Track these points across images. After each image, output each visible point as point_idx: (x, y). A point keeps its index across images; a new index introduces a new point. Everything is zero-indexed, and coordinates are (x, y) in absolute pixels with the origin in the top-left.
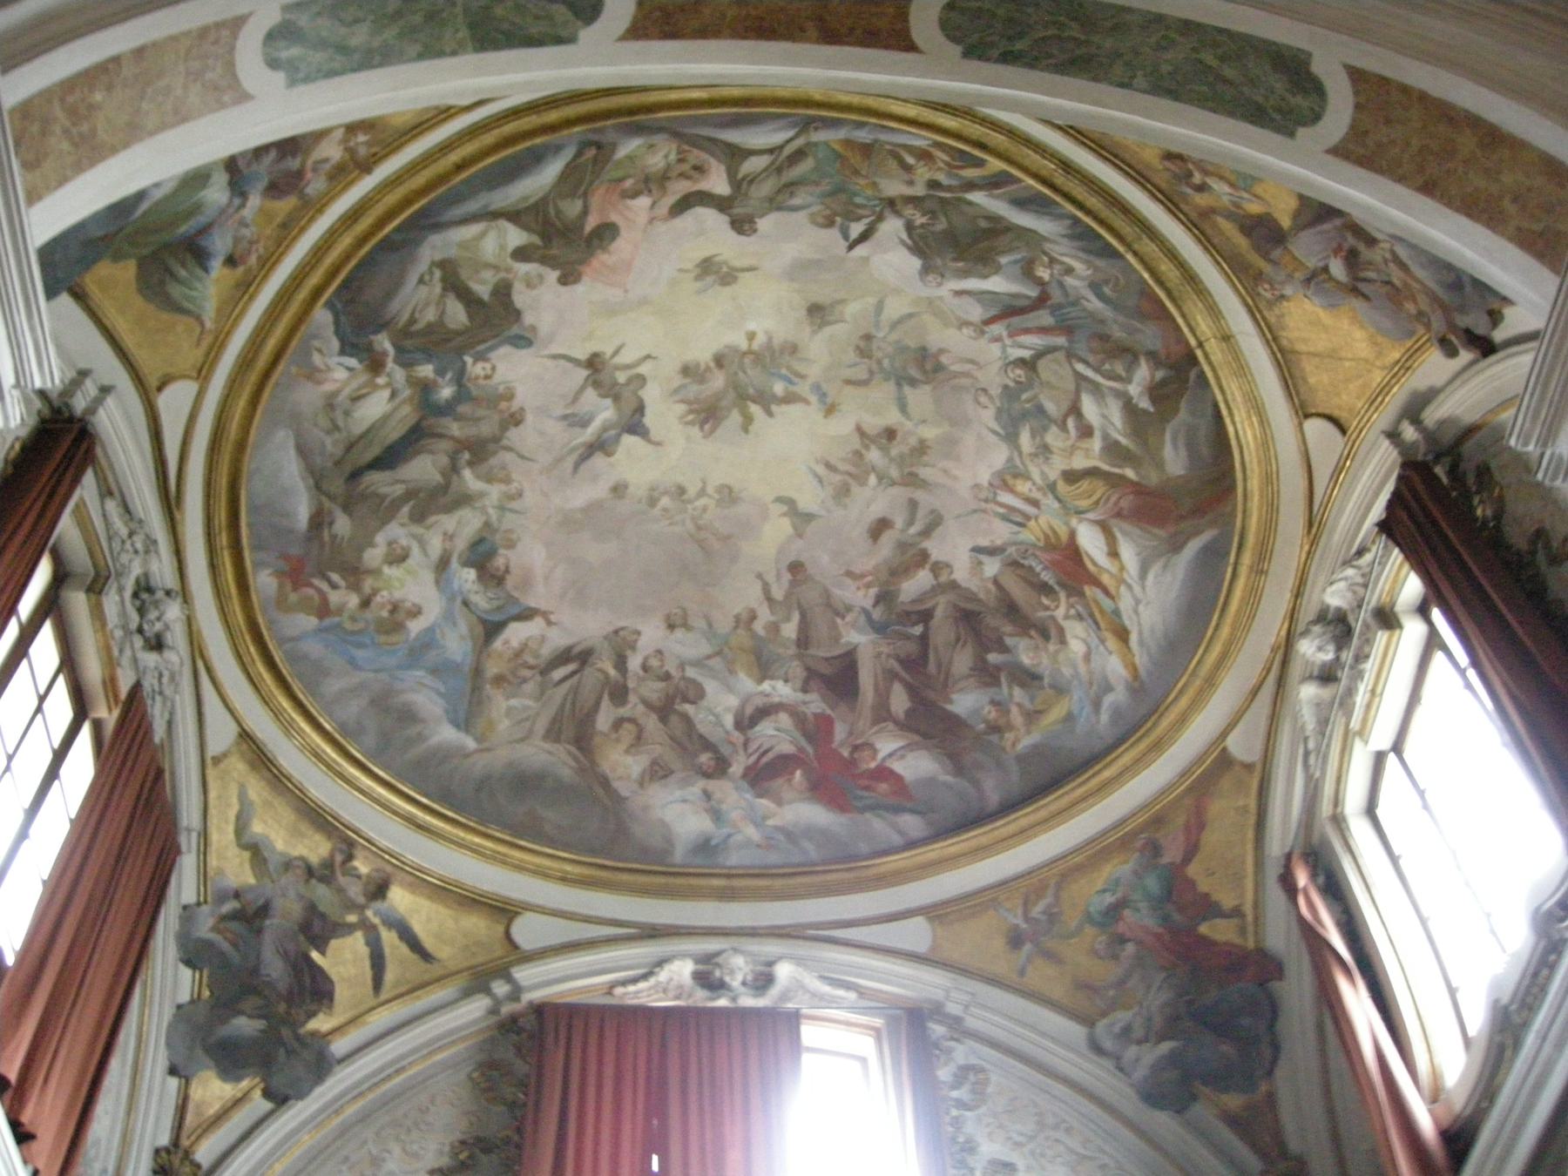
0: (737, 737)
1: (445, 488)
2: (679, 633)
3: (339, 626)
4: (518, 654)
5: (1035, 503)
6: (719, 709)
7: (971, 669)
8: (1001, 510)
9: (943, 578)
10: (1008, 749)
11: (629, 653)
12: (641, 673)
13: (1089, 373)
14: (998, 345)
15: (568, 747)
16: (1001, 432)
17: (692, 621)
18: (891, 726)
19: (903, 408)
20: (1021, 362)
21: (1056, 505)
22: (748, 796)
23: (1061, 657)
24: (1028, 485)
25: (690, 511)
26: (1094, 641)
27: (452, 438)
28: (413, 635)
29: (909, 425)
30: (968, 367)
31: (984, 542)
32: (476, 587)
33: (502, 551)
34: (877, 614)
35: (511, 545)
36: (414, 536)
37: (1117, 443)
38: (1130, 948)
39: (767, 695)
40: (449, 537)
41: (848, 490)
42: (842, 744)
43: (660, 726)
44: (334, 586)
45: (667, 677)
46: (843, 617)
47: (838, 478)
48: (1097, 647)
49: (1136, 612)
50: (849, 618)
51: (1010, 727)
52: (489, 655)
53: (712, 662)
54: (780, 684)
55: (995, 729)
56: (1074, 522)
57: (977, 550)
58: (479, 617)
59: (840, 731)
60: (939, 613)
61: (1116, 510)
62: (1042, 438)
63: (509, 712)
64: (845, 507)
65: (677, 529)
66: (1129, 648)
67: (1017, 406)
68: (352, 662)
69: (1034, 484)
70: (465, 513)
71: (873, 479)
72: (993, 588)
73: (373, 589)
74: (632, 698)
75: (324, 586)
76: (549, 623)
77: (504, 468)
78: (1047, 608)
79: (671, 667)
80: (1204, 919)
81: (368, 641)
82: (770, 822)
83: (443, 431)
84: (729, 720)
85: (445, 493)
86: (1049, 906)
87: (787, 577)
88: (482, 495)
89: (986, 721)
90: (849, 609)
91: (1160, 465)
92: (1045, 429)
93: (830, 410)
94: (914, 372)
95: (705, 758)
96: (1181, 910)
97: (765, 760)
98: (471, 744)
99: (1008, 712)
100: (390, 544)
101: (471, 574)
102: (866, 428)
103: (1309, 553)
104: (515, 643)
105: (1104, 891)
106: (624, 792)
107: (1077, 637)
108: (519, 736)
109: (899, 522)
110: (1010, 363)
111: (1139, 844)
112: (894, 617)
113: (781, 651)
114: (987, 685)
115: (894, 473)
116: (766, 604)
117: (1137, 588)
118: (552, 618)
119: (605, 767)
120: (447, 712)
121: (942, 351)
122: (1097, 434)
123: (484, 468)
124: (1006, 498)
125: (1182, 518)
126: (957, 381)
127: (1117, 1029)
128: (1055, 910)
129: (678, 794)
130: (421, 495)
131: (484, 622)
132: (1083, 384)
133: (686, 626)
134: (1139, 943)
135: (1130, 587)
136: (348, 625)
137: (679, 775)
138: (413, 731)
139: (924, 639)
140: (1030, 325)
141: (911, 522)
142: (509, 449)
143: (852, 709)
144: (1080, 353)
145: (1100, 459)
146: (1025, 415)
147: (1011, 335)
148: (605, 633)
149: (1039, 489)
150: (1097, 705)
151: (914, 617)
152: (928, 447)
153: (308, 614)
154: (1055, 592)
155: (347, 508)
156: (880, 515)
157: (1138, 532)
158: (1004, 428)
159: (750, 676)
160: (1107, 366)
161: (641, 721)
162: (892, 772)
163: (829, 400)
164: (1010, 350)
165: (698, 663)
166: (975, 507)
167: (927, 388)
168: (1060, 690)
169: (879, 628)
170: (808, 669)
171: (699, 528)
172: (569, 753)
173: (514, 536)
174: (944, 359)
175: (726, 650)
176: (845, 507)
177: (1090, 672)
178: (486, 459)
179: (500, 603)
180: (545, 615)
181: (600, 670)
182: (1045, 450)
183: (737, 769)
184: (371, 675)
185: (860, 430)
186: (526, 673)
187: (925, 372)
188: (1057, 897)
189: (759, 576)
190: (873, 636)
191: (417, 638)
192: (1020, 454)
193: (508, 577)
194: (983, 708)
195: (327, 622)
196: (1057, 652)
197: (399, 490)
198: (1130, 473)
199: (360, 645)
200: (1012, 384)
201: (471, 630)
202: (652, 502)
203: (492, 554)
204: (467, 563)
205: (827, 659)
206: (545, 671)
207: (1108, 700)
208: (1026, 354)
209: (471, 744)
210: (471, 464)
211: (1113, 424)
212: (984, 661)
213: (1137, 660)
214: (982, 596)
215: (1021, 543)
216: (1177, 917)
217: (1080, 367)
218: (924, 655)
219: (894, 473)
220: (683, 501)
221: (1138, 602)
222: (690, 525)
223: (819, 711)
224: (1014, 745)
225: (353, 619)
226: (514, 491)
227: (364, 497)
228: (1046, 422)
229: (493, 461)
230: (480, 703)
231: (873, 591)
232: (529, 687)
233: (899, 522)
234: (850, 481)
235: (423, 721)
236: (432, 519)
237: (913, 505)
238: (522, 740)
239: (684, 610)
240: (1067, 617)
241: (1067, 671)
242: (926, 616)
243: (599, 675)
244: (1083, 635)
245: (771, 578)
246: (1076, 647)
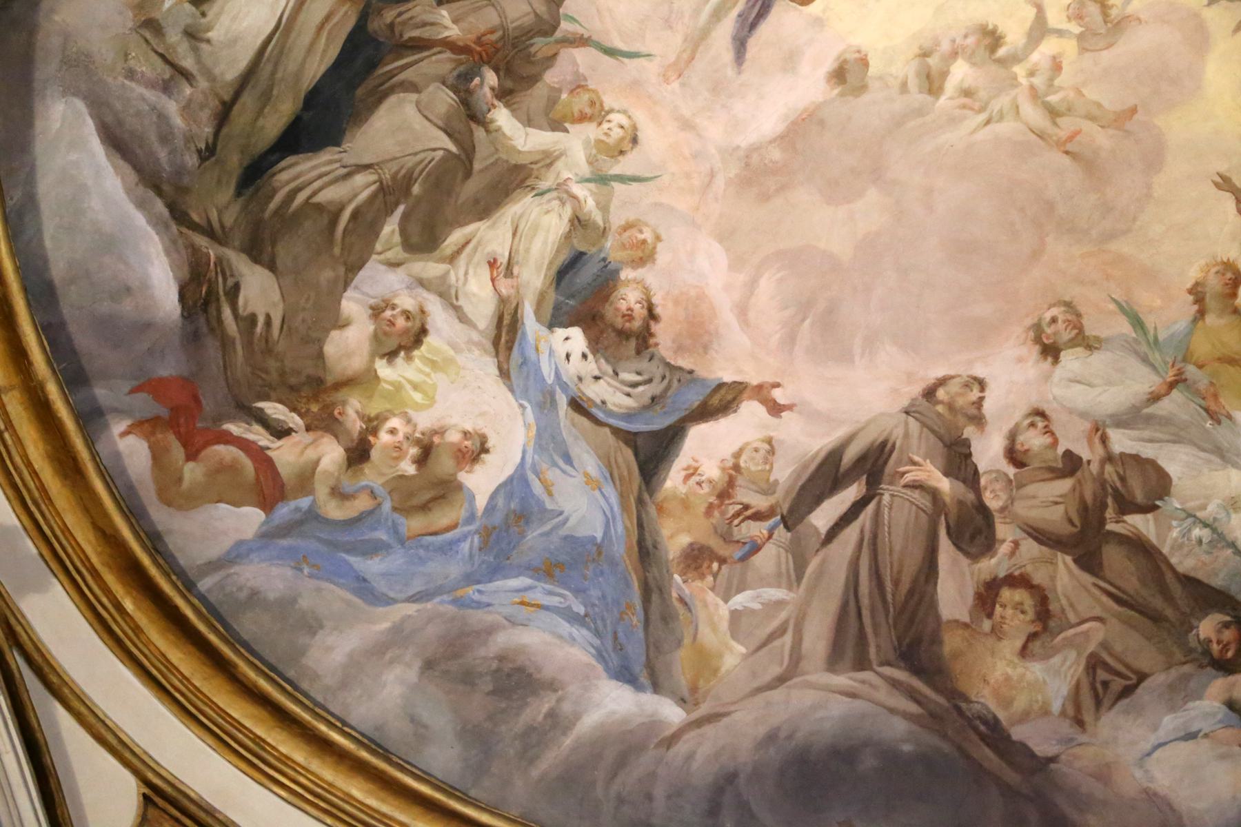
1: (464, 160)
2: (1071, 360)
3: (312, 516)
4: (724, 494)
6: (1212, 509)
11: (969, 432)
12: (1011, 471)
15: (887, 671)
17: (1092, 328)
25: (1023, 81)
27: (449, 45)
28: (481, 502)
32: (591, 367)
33: (626, 274)
35: (644, 256)
36: (422, 283)
40: (502, 268)
43: (1087, 578)
44: (281, 432)
45: (1072, 464)
52: (660, 509)
58: (616, 431)
63: (735, 616)
65: (1006, 128)
68: (364, 589)
70: (522, 207)
73: (368, 420)
74: (1005, 531)
75: (258, 435)
76: (776, 409)
77: (579, 86)
79: (1074, 439)
81: (382, 535)
83: (425, 33)
85: (468, 174)
88: (549, 159)
95: (1208, 627)
98: (672, 713)
100: (376, 312)
101: (575, 339)
104: (712, 471)
106: (1042, 748)
108: (776, 670)
118: (779, 395)
119: (984, 698)
120: (600, 656)
123: (536, 96)
129: (1170, 723)
130: (416, 189)
131: (629, 438)
133: (1089, 344)
136: (334, 511)
137: (1159, 679)
138: (537, 710)
142: (581, 41)
148: (905, 402)
153: (236, 504)
155: (257, 250)
161: (1039, 577)
165: (1130, 418)
171: (1053, 113)
172: (894, 684)
173: (647, 235)
175: (1191, 370)
178: (534, 79)
179: (655, 388)
180: (761, 393)
181: (916, 486)
184: (411, 609)
186: (757, 530)
191: (490, 508)
193: (655, 328)
195: (284, 511)
197: (362, 186)
199: (373, 549)
201: (608, 463)
202: (932, 83)
203: (607, 282)
204: (557, 319)
206: (793, 517)
209: (672, 713)
210: (504, 94)
220: (1002, 62)
222: (1032, 114)
225: (338, 493)
226: (617, 133)
227: (288, 220)
229: (551, 77)
230: (668, 618)
232: (769, 558)
235: (552, 686)
236: (455, 237)
238: (781, 680)
239: (1068, 305)
243: (916, 495)
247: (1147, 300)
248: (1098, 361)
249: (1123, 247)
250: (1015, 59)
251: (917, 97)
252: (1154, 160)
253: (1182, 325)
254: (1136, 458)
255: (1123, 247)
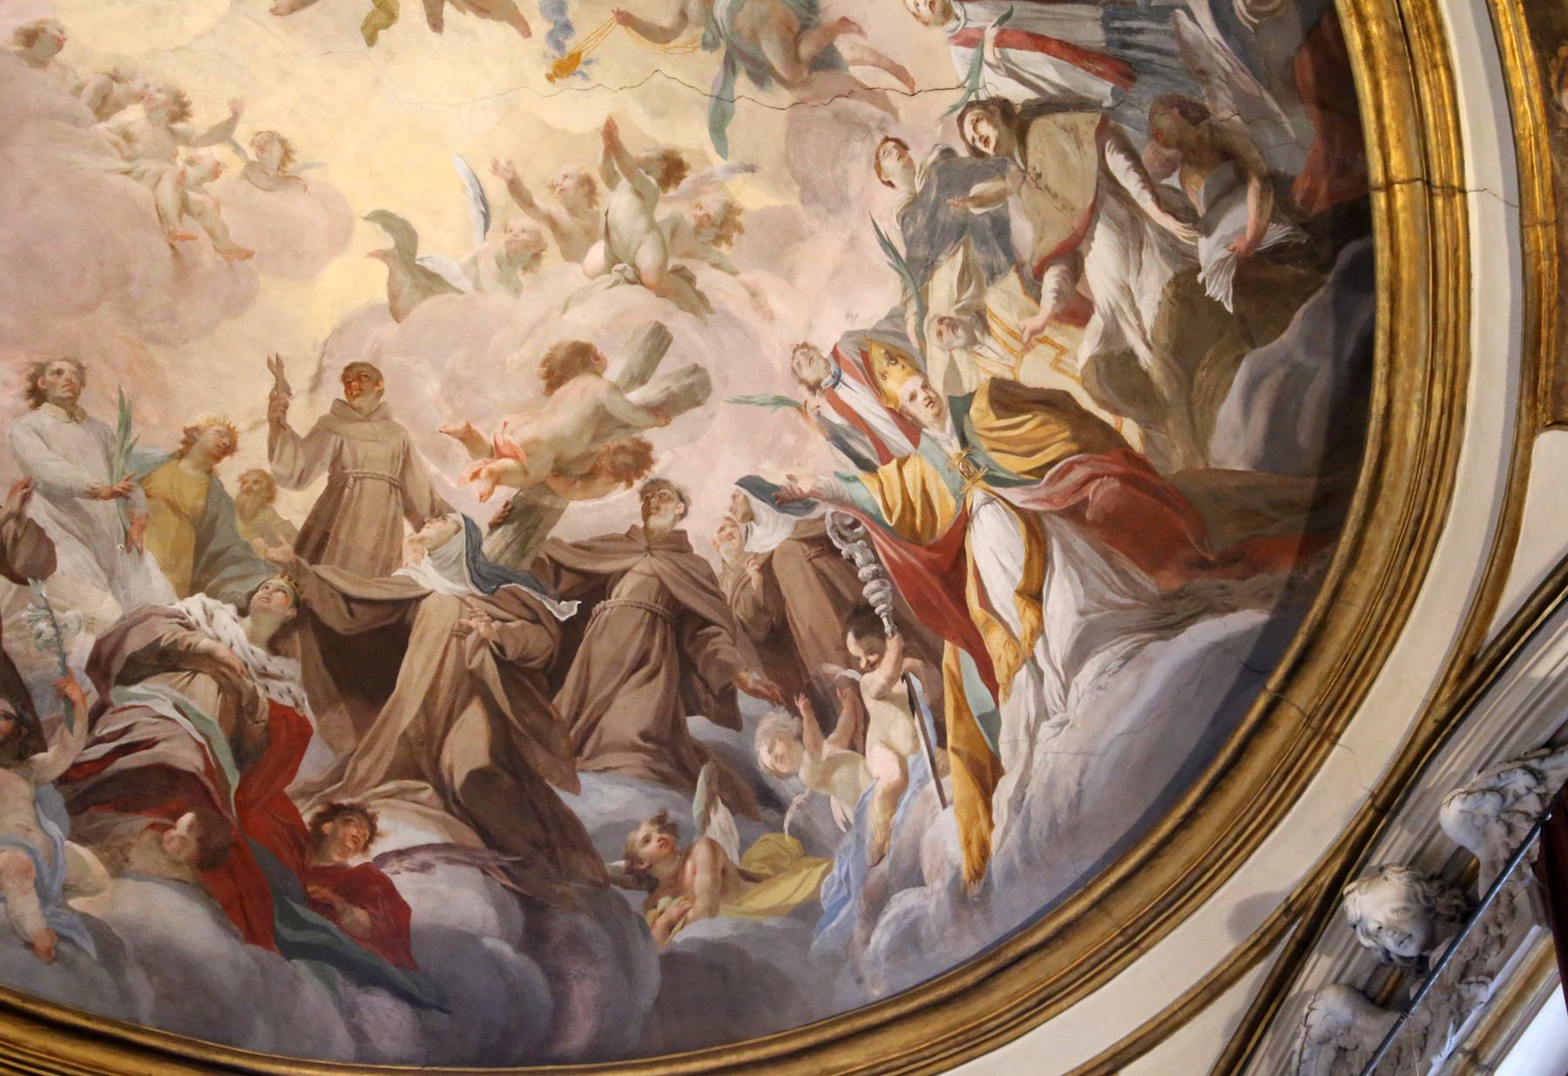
0: (85, 691)
2: (48, 416)
5: (912, 429)
6: (68, 616)
7: (645, 736)
8: (837, 419)
9: (659, 522)
10: (657, 932)
13: (1131, 182)
14: (969, 52)
16: (903, 252)
18: (428, 793)
19: (719, 125)
20: (1001, 110)
21: (954, 448)
22: (55, 829)
23: (840, 775)
24: (915, 383)
25: (180, 162)
26: (920, 764)
29: (718, 163)
30: (886, 80)
31: (775, 475)
34: (492, 545)
37: (1130, 355)
39: (188, 627)
41: (537, 256)
42: (306, 794)
46: (419, 526)
47: (523, 221)
48: (922, 782)
49: (1032, 734)
50: (431, 530)
51: (676, 886)
53: (96, 508)
54: (225, 614)
55: (644, 879)
56: (977, 495)
57: (755, 485)
59: (314, 764)
60: (623, 590)
61: (1071, 502)
62: (981, 292)
64: (517, 291)
65: (139, 189)
66: (988, 807)
67: (954, 206)
69: (925, 386)
71: (597, 254)
72: (752, 572)
78: (850, 662)
82: (76, 903)
84: (81, 647)
87: (335, 390)
89: (632, 858)
90: (439, 511)
91: (1199, 435)
92: (993, 275)
93: (566, 67)
94: (772, 52)
97: (124, 762)
99: (687, 853)
102: (625, 137)
103: (1442, 724)
107: (888, 745)
109: (616, 368)
110: (982, 105)
112: (526, 565)
113: (258, 542)
114: (665, 780)
115: (647, 257)
116: (265, 429)
117: (1052, 683)
121: (845, 24)
122: (1097, 322)
124: (855, 395)
125: (1204, 565)
126: (851, 103)
132: (1111, 202)
135: (1039, 676)
139: (572, 632)
140: (1051, 31)
141: (640, 378)
143: (360, 729)
144: (1128, 130)
145: (1083, 381)
146: (961, 230)
147: (1000, 42)
149: (931, 402)
150: (875, 905)
151: (567, 581)
152: (740, 229)
154: (883, 636)
156: (583, 338)
157: (1100, 564)
158: (909, 243)
159: (166, 568)
160: (1174, 181)
162: (390, 892)
163: (571, 45)
164: (987, 73)
165: (61, 497)
166: (783, 393)
167: (785, 97)
168: (811, 846)
169: (486, 577)
170: (299, 603)
171: (185, 207)
174: (845, 46)
175: (139, 494)
176: (517, 291)
177: (888, 829)
182: (976, 321)
183: (54, 759)
185: (610, 134)
187: (794, 59)
189: (276, 366)
190: (465, 588)
192: (923, 310)
194: (636, 825)
196: (833, 763)
198: (1131, 431)
200: (963, 152)
202: (104, 105)
205: (348, 599)
207: (904, 901)
208: (1018, 94)
211: (1137, 314)
212: (678, 727)
213: (995, 838)
214: (726, 588)
215: (851, 504)
217: (1118, 164)
218: (554, 674)
219: (647, 257)
220: (173, 133)
221: (1043, 714)
222: (168, 195)
223: (288, 702)
224: (670, 927)
228: (1003, 258)
231: (504, 494)
233: (616, 368)
234: (547, 235)
237: (660, 340)
239: (81, 370)
240: (882, 696)
241: (841, 810)
242: (595, 588)
244: (904, 745)
245: (298, 380)
246: (880, 765)
247: (147, 412)
248: (71, 433)
249: (161, 356)
250: (186, 140)
251: (83, 108)
252: (237, 305)
253: (160, 453)
254: (40, 532)
255: (161, 356)
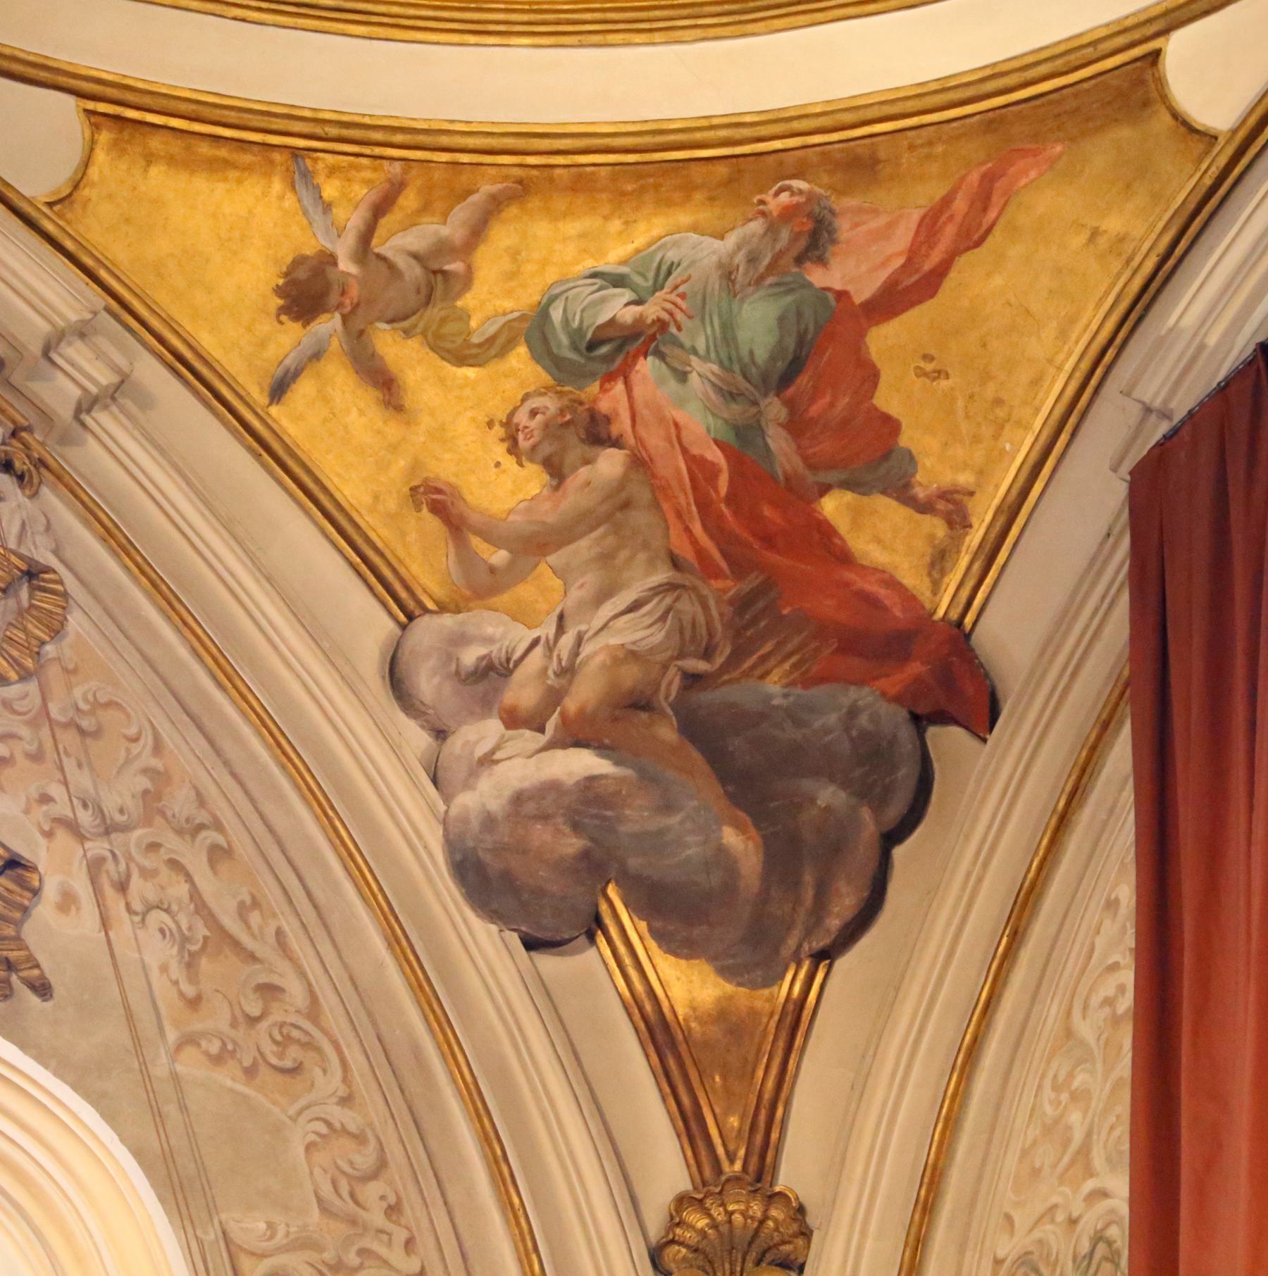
38: (610, 464)
80: (847, 485)
86: (443, 248)
96: (796, 426)
105: (618, 281)
111: (776, 202)
127: (470, 656)
128: (455, 266)
134: (640, 463)
188: (477, 233)
216: (778, 442)
